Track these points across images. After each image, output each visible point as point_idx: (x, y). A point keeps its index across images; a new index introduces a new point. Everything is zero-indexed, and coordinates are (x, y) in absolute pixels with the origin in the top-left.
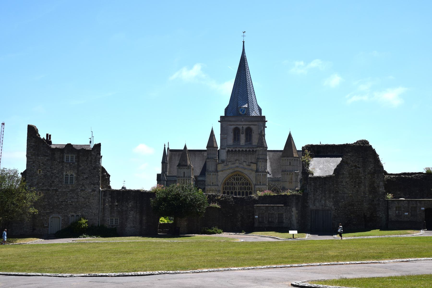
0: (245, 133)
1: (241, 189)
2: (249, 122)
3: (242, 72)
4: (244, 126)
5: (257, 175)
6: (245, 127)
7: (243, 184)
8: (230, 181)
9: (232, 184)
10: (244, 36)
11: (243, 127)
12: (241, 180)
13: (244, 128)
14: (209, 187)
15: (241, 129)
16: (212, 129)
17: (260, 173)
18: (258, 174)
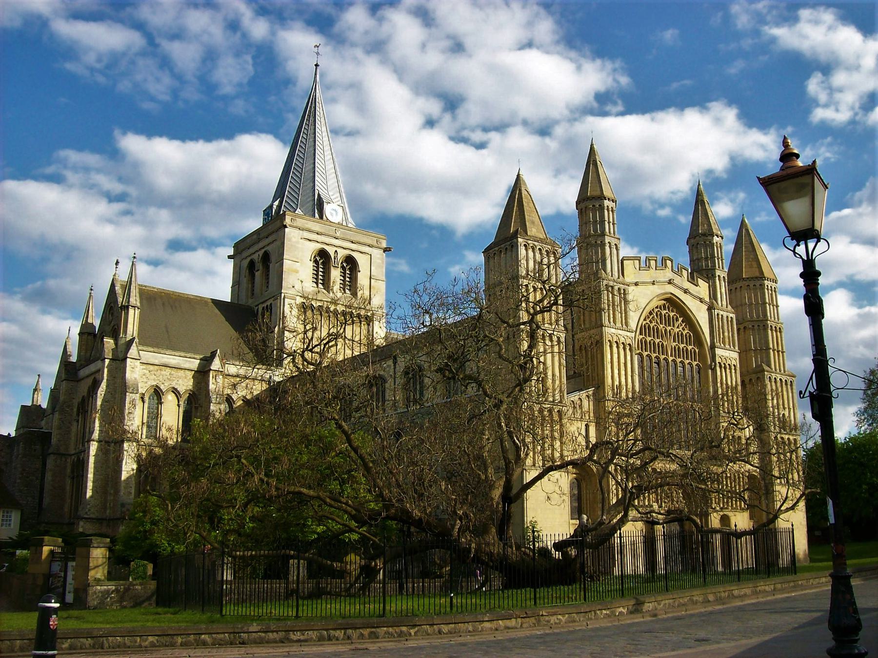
0: (339, 266)
1: (677, 352)
2: (352, 242)
3: (320, 128)
4: (339, 250)
5: (716, 316)
6: (342, 253)
7: (679, 337)
8: (651, 322)
9: (657, 333)
10: (318, 54)
11: (336, 251)
12: (676, 326)
13: (339, 256)
14: (613, 330)
15: (333, 257)
16: (592, 145)
17: (721, 313)
18: (718, 314)
